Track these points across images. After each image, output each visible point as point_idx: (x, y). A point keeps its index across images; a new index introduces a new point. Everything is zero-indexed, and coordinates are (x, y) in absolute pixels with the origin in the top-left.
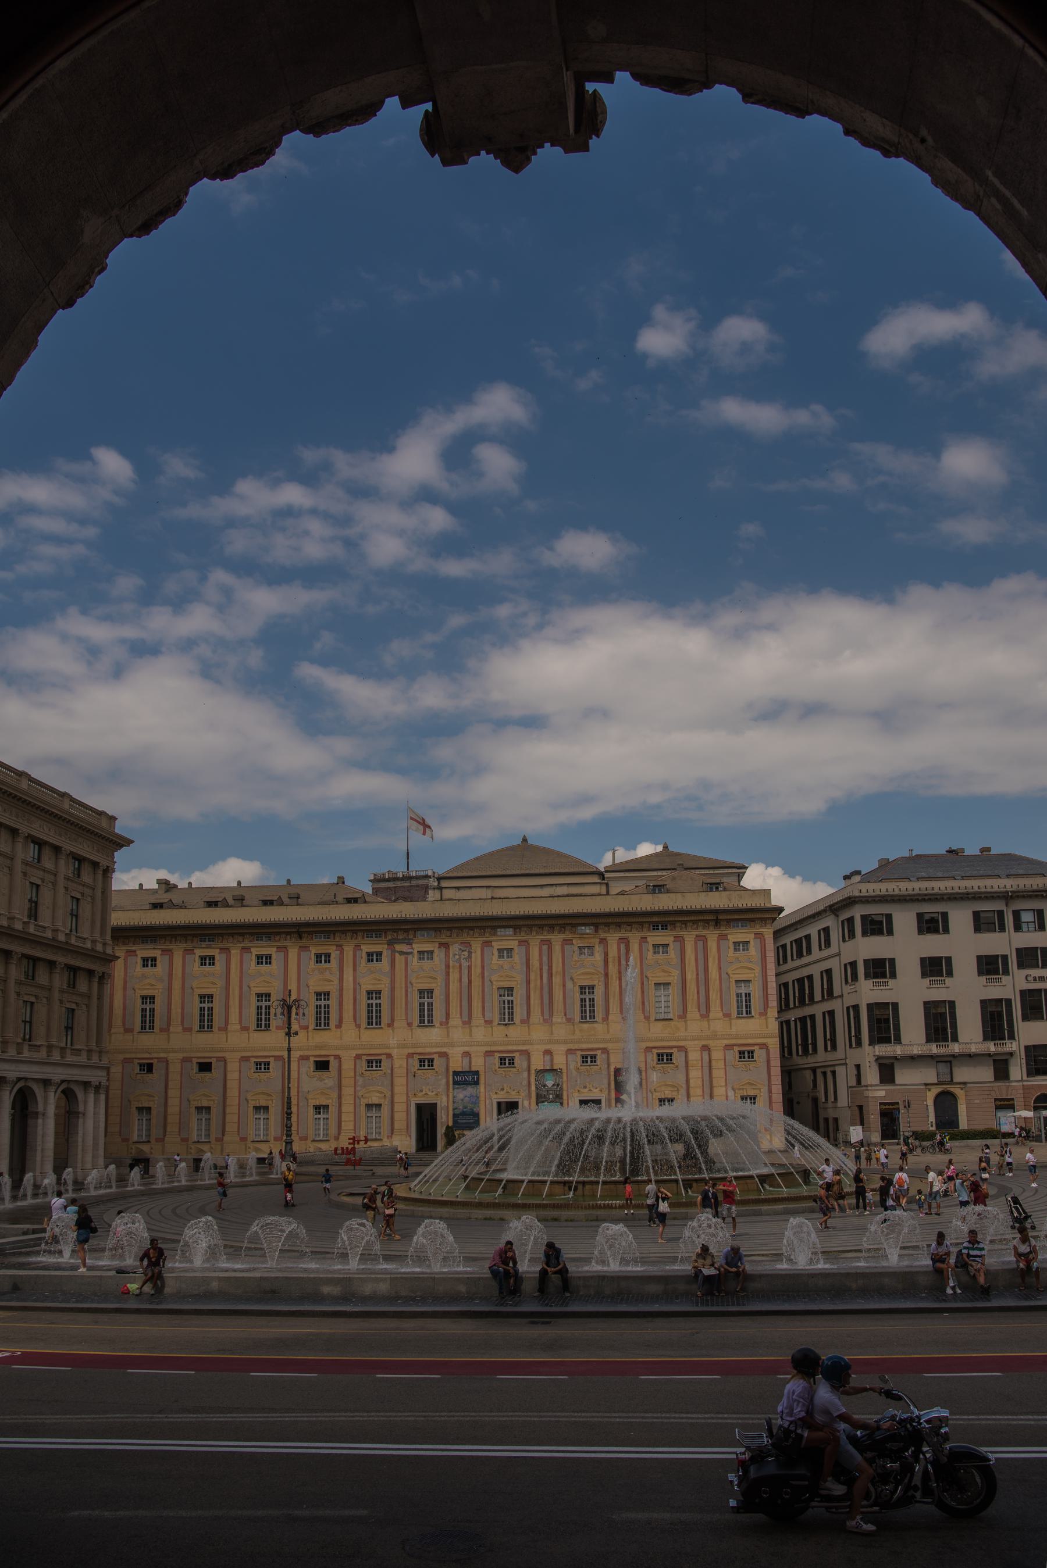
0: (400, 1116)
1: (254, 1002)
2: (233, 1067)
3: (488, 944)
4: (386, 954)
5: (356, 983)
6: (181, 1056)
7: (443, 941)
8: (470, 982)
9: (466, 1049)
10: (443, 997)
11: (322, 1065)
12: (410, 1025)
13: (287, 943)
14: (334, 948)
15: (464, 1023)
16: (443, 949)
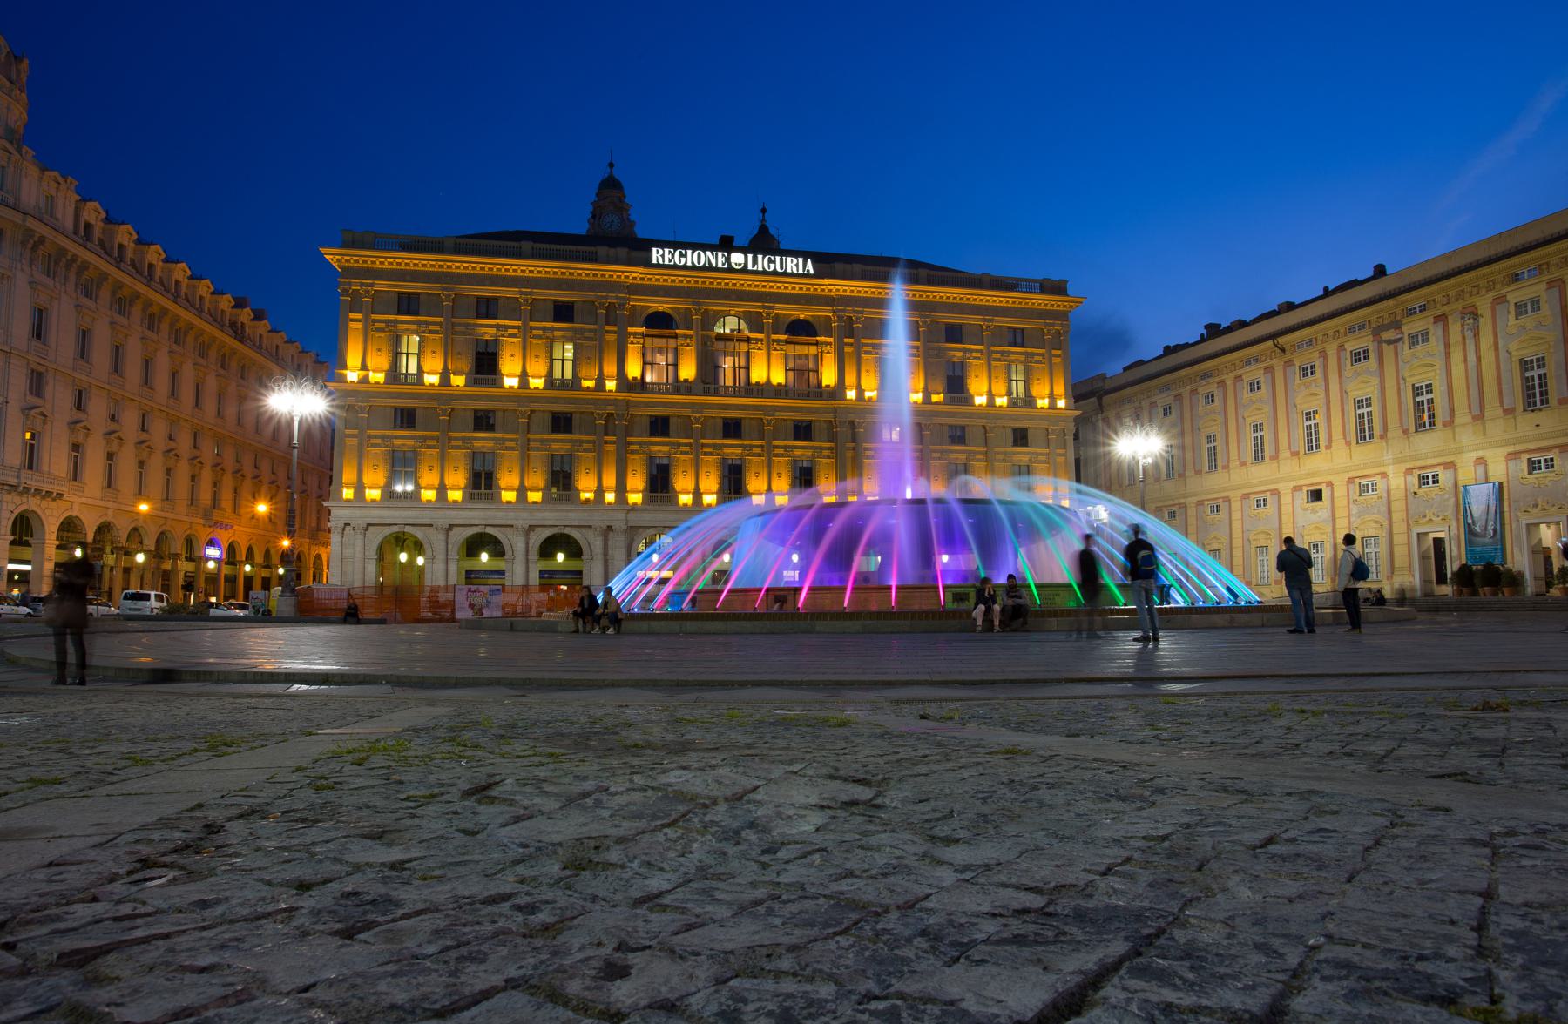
0: (1400, 551)
1: (1250, 435)
2: (1236, 505)
3: (1501, 300)
4: (1372, 347)
5: (1343, 392)
6: (1195, 499)
7: (1439, 313)
8: (1479, 359)
9: (1480, 454)
10: (1444, 388)
11: (1317, 495)
12: (1405, 432)
13: (1273, 362)
14: (1317, 354)
15: (1475, 418)
16: (1440, 325)
